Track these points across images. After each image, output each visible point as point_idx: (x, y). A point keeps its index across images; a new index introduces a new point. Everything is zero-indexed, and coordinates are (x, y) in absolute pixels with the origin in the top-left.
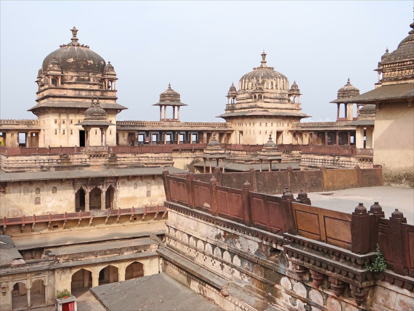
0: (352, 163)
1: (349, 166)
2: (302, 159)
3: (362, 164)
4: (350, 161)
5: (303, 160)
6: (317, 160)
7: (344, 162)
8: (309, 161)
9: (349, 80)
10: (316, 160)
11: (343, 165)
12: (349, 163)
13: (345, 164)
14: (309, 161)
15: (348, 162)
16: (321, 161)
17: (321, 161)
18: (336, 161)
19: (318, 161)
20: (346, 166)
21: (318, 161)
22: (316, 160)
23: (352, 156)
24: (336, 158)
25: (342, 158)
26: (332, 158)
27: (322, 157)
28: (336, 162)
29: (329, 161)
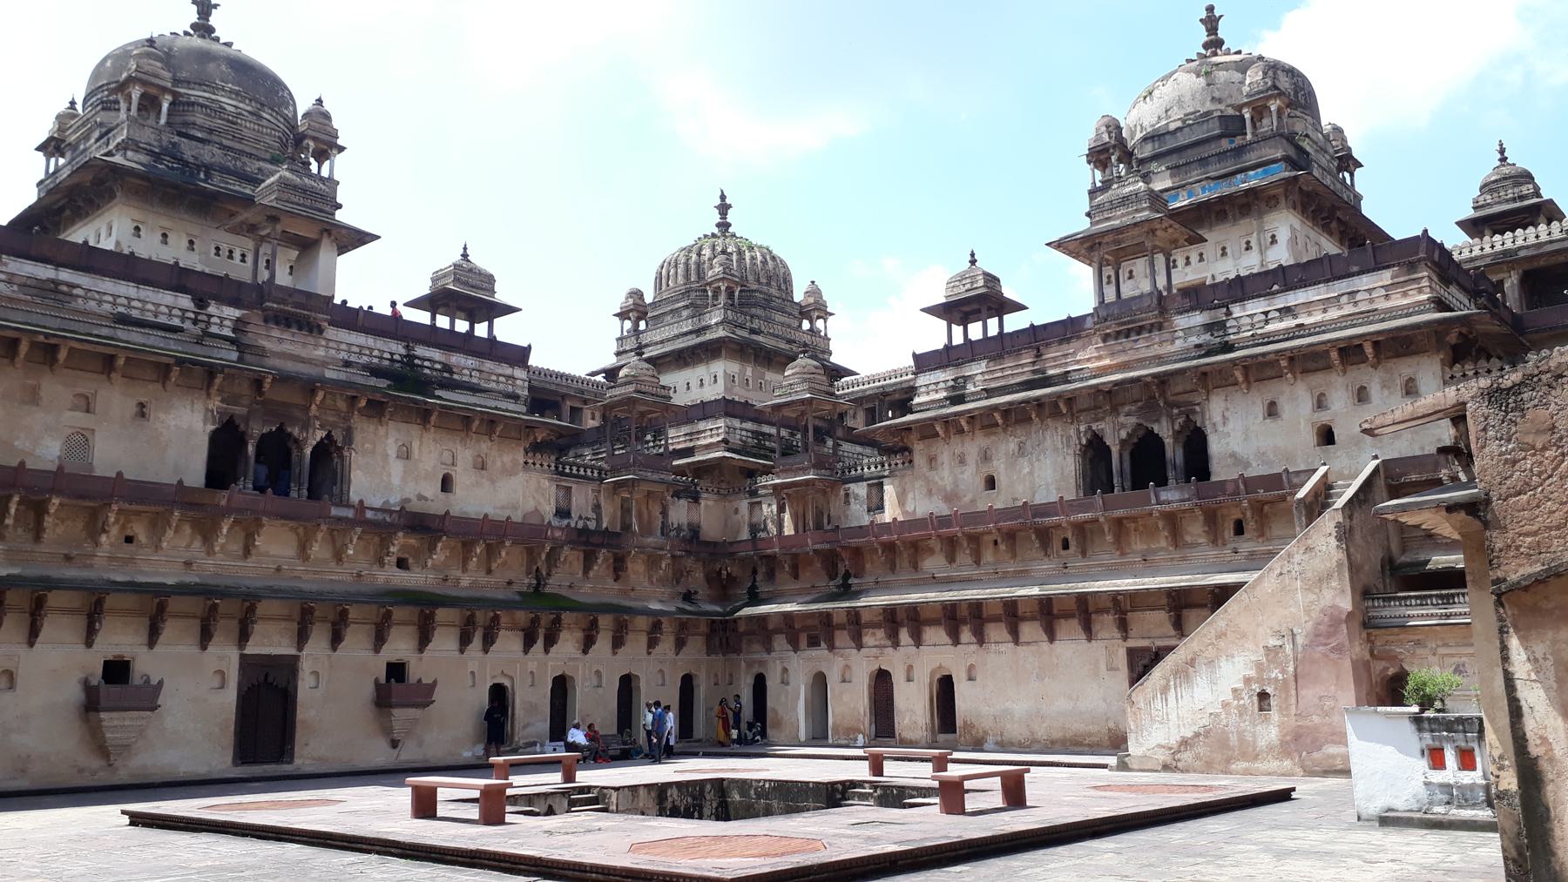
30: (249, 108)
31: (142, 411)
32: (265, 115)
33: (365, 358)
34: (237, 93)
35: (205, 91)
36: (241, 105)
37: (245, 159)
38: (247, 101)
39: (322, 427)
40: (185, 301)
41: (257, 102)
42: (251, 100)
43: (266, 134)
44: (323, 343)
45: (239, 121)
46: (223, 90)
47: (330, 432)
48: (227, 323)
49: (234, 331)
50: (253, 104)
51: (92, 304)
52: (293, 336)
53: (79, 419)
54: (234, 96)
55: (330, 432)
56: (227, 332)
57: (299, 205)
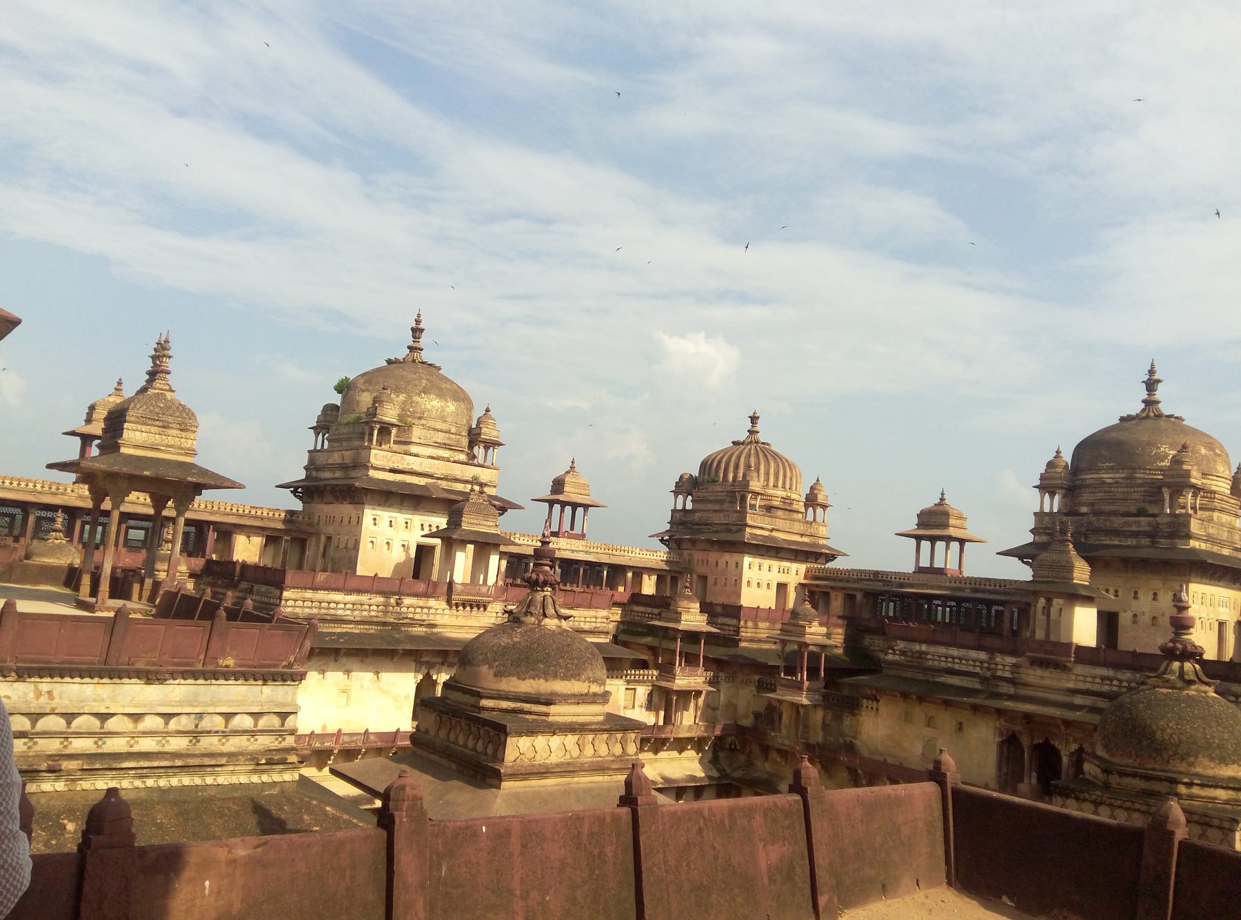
0: (432, 611)
1: (424, 617)
2: (287, 600)
3: (455, 611)
4: (427, 608)
5: (290, 603)
6: (337, 603)
7: (411, 610)
8: (310, 608)
9: (120, 383)
10: (332, 605)
11: (410, 616)
12: (425, 611)
13: (415, 613)
14: (310, 608)
15: (422, 608)
16: (349, 606)
17: (350, 606)
18: (393, 607)
19: (341, 606)
20: (417, 617)
21: (341, 606)
22: (332, 605)
23: (432, 597)
24: (392, 601)
25: (407, 601)
26: (380, 599)
27: (353, 598)
28: (391, 608)
29: (374, 607)
30: (1123, 475)
31: (960, 727)
32: (1138, 475)
33: (1107, 687)
34: (1112, 468)
35: (1093, 474)
36: (1117, 475)
37: (1113, 518)
38: (1121, 471)
39: (1075, 741)
40: (983, 656)
41: (1128, 469)
42: (1123, 469)
43: (1134, 492)
44: (1073, 677)
45: (1113, 489)
46: (1104, 469)
47: (1081, 745)
48: (1007, 668)
49: (1012, 673)
50: (1126, 471)
51: (936, 663)
52: (1051, 673)
53: (929, 732)
54: (1110, 471)
55: (1081, 745)
56: (1008, 675)
57: (1048, 577)
